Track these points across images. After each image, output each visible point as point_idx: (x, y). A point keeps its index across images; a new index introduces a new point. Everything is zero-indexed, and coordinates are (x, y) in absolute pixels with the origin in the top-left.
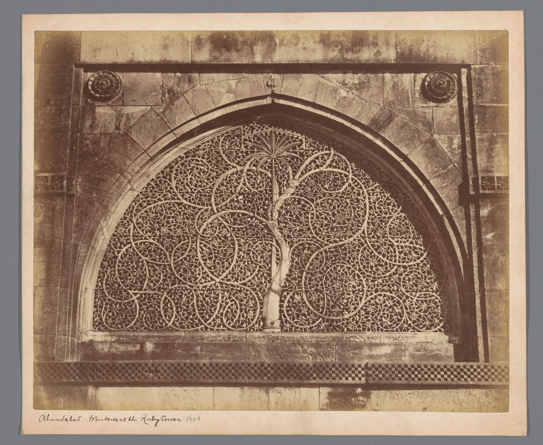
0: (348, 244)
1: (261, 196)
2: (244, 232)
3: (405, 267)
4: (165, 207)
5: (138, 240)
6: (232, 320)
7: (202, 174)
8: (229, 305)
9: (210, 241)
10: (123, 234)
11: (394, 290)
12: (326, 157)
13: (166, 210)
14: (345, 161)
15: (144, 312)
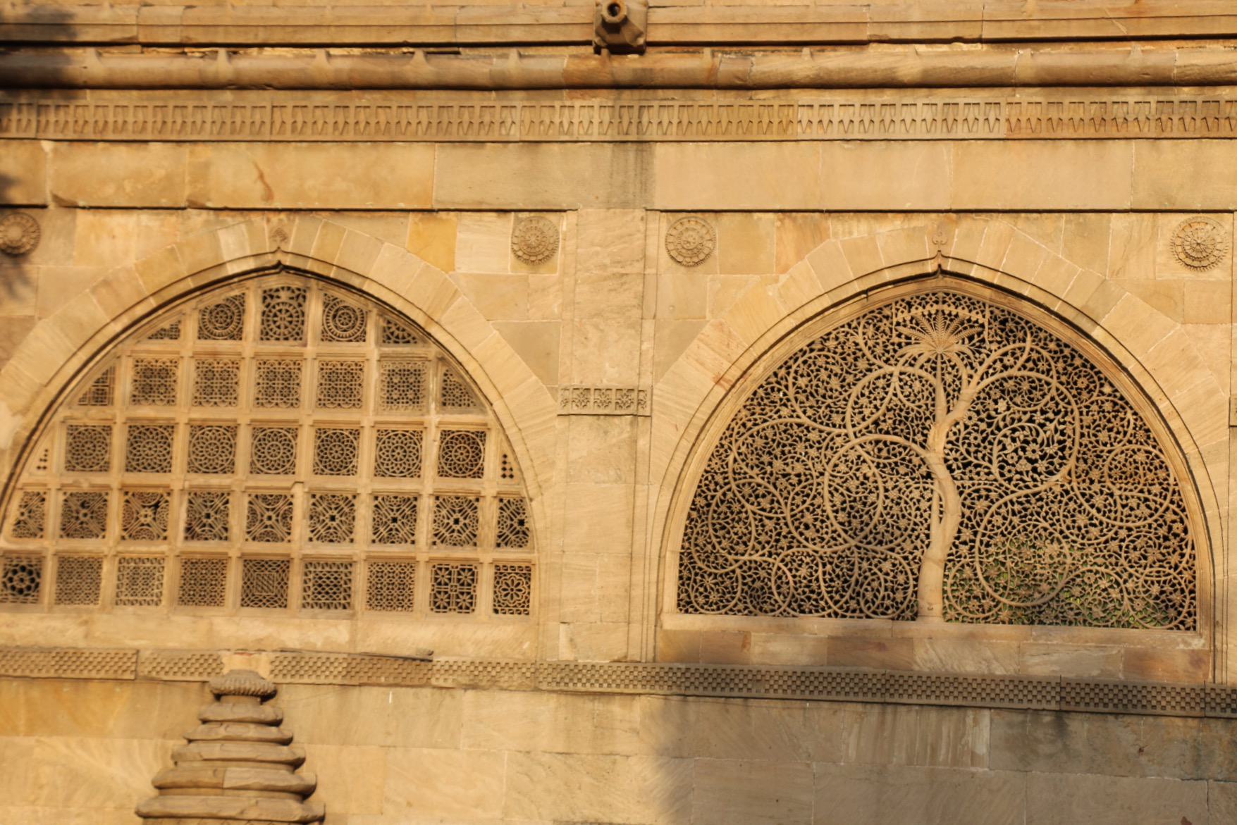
1: (919, 413)
2: (892, 469)
3: (1129, 529)
6: (874, 603)
8: (869, 579)
9: (844, 482)
11: (1111, 564)
12: (1018, 353)
14: (1047, 360)
15: (750, 587)
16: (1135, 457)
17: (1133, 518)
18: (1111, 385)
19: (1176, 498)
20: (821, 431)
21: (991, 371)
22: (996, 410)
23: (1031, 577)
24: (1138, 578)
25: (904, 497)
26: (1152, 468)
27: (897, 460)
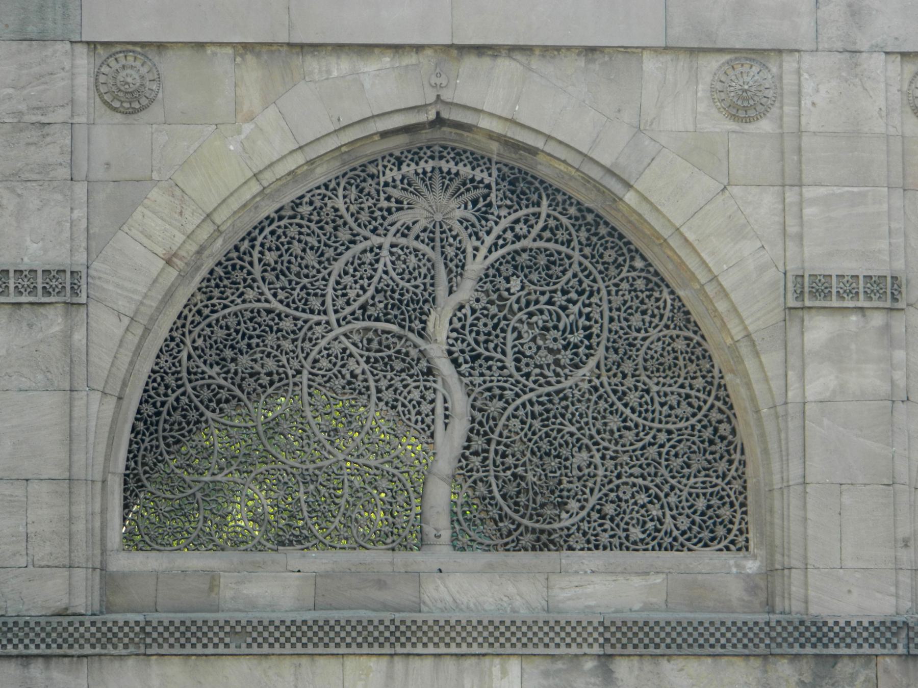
0: (571, 388)
2: (386, 365)
3: (669, 432)
4: (243, 317)
5: (197, 380)
7: (308, 250)
9: (326, 382)
10: (170, 369)
11: (649, 475)
12: (532, 220)
13: (245, 323)
14: (567, 229)
16: (674, 345)
17: (673, 419)
18: (643, 258)
19: (722, 393)
20: (296, 319)
21: (501, 242)
22: (508, 290)
23: (557, 493)
24: (681, 491)
25: (401, 398)
26: (693, 357)
27: (391, 352)
